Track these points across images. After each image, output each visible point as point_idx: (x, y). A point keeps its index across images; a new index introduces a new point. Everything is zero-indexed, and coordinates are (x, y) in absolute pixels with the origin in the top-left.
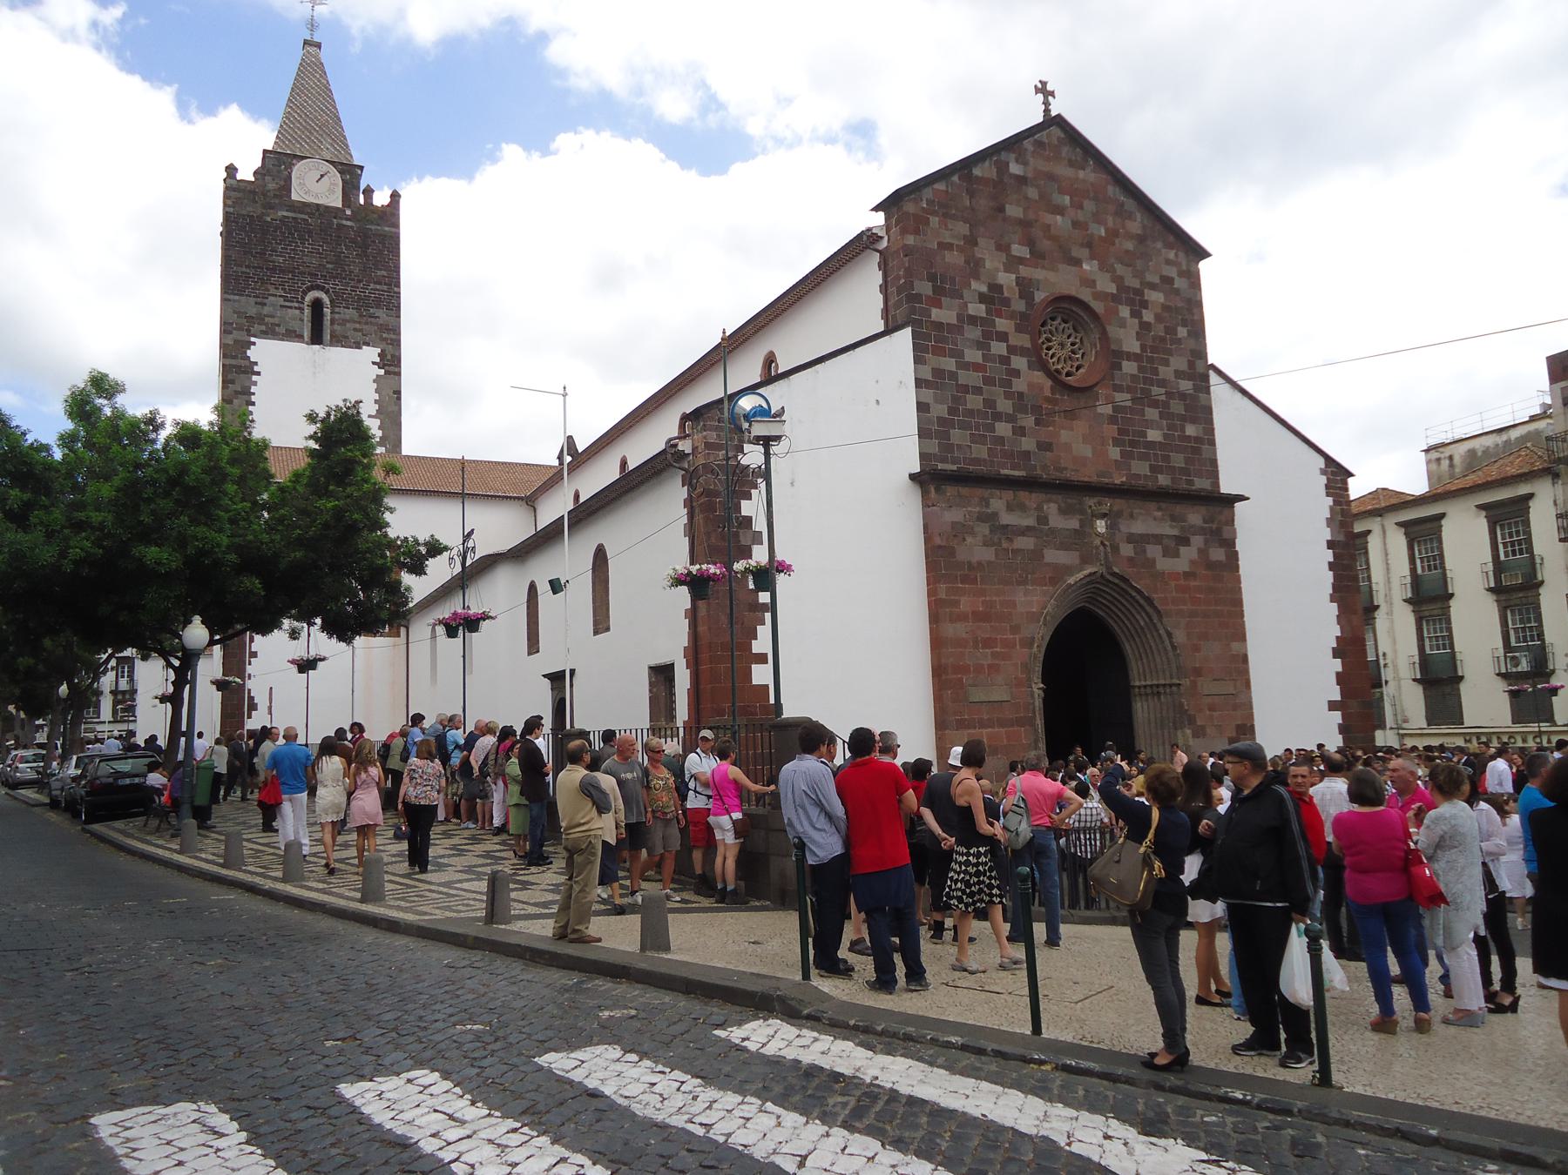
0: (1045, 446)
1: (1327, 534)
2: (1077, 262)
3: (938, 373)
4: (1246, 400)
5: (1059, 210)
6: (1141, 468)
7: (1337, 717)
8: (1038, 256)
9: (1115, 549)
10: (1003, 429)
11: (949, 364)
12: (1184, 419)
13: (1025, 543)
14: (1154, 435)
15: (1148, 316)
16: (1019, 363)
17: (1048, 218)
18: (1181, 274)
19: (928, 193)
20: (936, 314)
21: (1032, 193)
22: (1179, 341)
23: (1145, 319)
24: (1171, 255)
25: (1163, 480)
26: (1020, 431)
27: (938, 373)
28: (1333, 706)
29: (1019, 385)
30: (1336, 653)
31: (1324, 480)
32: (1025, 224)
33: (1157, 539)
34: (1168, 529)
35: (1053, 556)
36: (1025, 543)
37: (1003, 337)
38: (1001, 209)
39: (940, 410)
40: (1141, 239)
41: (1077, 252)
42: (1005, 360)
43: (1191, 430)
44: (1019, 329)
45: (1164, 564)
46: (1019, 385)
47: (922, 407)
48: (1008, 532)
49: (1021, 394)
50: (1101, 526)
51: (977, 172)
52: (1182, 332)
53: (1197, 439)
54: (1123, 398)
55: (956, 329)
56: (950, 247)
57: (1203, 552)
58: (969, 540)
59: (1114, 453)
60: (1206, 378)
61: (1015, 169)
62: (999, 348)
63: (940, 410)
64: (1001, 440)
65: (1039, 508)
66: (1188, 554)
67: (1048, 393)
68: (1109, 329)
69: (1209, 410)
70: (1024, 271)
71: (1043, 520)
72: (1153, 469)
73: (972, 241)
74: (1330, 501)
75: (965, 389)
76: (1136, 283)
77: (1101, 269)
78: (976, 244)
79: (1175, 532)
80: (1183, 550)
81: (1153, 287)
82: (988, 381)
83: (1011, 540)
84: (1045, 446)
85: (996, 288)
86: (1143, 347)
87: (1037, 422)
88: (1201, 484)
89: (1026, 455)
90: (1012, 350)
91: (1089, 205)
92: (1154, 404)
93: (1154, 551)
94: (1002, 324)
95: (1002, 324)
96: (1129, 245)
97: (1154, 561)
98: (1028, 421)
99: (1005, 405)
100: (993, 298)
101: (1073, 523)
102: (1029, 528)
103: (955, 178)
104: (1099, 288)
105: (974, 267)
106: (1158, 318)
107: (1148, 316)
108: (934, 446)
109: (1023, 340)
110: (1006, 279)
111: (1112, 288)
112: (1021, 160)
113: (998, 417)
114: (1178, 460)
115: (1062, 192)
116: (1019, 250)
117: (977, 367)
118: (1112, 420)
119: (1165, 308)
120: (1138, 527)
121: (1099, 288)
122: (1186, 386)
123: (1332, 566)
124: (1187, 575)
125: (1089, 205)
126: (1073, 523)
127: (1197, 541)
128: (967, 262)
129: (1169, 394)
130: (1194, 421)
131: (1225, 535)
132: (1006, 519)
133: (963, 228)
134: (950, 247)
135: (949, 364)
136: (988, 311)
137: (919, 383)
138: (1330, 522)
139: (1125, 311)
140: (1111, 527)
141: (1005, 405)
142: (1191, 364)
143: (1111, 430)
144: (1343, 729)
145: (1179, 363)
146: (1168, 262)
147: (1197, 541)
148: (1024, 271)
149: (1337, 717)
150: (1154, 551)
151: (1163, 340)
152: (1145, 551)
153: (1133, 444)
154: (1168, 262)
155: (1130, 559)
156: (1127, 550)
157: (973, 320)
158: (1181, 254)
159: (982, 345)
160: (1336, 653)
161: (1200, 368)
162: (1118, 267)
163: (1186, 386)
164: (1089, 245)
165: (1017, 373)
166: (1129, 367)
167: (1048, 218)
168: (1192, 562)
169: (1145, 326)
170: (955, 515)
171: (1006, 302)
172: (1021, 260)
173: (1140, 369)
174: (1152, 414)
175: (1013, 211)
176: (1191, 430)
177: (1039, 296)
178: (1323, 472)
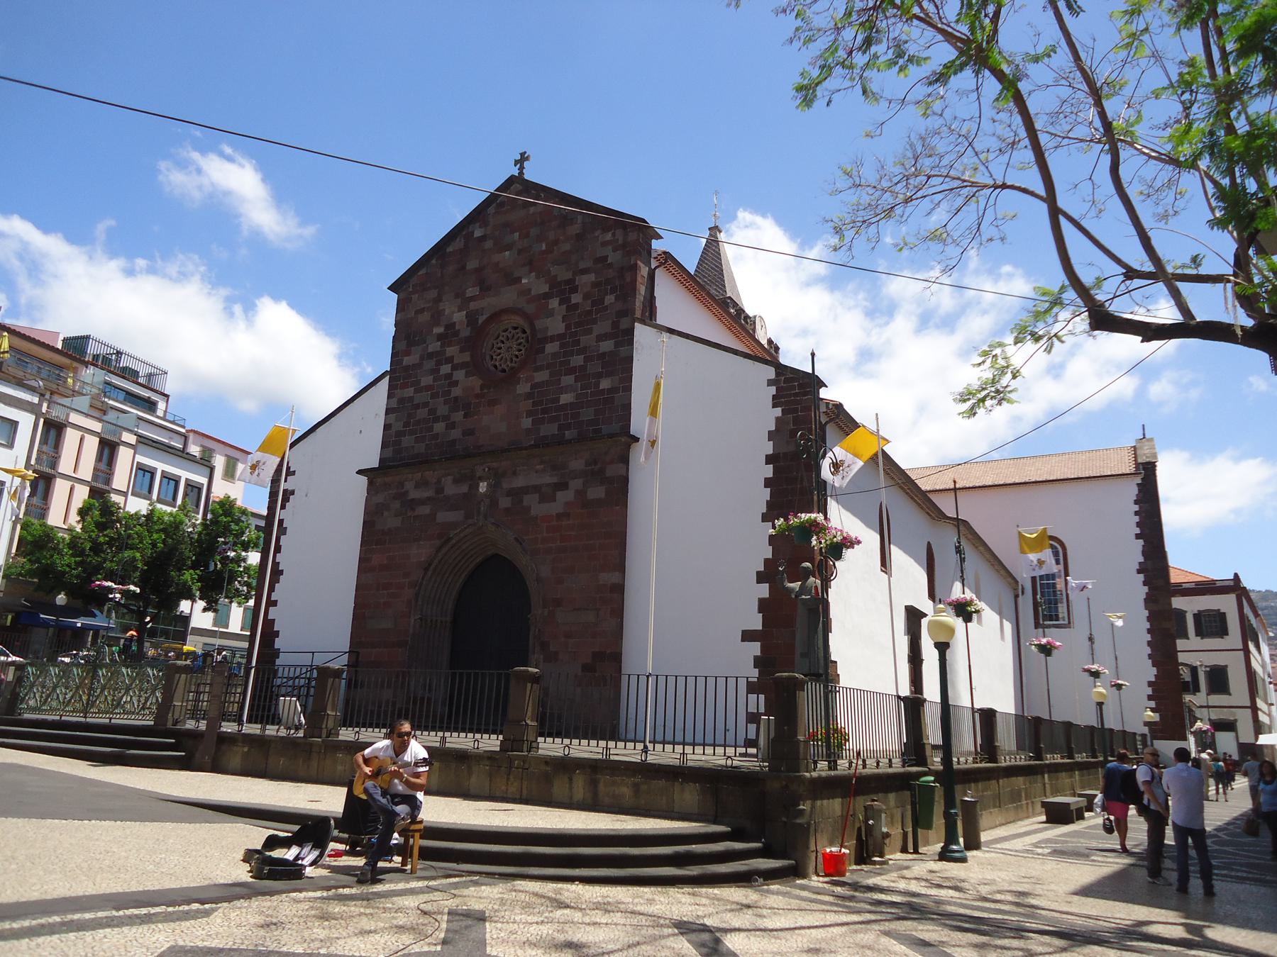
0: (469, 432)
1: (769, 448)
2: (519, 279)
3: (401, 401)
4: (675, 337)
5: (509, 247)
6: (550, 429)
7: (755, 648)
8: (485, 288)
9: (494, 503)
10: (439, 427)
11: (410, 392)
12: (600, 376)
13: (425, 510)
14: (566, 398)
15: (576, 298)
16: (459, 375)
17: (496, 257)
18: (615, 250)
19: (414, 280)
20: (407, 361)
21: (488, 244)
22: (606, 308)
23: (573, 301)
24: (609, 236)
25: (568, 434)
26: (452, 426)
27: (401, 401)
28: (748, 636)
29: (457, 392)
30: (761, 578)
31: (773, 390)
32: (478, 270)
33: (536, 489)
34: (548, 479)
35: (444, 516)
36: (425, 510)
37: (450, 360)
38: (463, 267)
39: (398, 426)
40: (580, 237)
41: (516, 275)
42: (449, 376)
43: (605, 384)
44: (462, 351)
45: (538, 509)
46: (457, 392)
47: (387, 427)
48: (413, 503)
49: (456, 398)
50: (483, 487)
51: (450, 249)
52: (610, 299)
53: (611, 391)
54: (541, 376)
55: (419, 365)
56: (422, 311)
57: (580, 494)
58: (386, 513)
59: (527, 423)
60: (630, 332)
61: (478, 233)
62: (445, 369)
63: (398, 426)
64: (436, 436)
65: (439, 481)
66: (564, 497)
67: (478, 391)
68: (539, 324)
69: (630, 359)
70: (473, 306)
71: (440, 490)
72: (560, 428)
73: (438, 300)
74: (778, 412)
75: (417, 407)
76: (568, 275)
77: (538, 277)
78: (441, 300)
79: (555, 480)
80: (560, 495)
81: (585, 271)
82: (434, 396)
83: (413, 510)
84: (469, 432)
85: (450, 326)
86: (568, 327)
87: (466, 416)
88: (605, 429)
89: (454, 441)
90: (454, 368)
91: (534, 231)
92: (571, 371)
93: (530, 500)
94: (451, 351)
95: (451, 351)
96: (566, 247)
97: (529, 508)
98: (458, 416)
99: (442, 410)
100: (450, 333)
101: (464, 489)
102: (429, 499)
103: (434, 261)
104: (533, 293)
105: (437, 317)
106: (586, 297)
107: (576, 298)
108: (389, 452)
109: (466, 357)
110: (459, 317)
111: (545, 288)
112: (484, 224)
113: (436, 420)
114: (587, 414)
115: (513, 232)
116: (471, 291)
117: (428, 388)
118: (529, 396)
119: (595, 285)
120: (519, 482)
121: (533, 293)
122: (607, 346)
123: (768, 483)
124: (559, 516)
125: (534, 231)
126: (464, 489)
127: (576, 484)
128: (432, 316)
129: (587, 359)
130: (609, 374)
131: (611, 471)
132: (414, 494)
133: (433, 294)
134: (422, 311)
135: (410, 392)
136: (442, 346)
137: (388, 412)
138: (771, 436)
139: (554, 303)
140: (493, 487)
141: (442, 410)
142: (615, 325)
143: (526, 405)
144: (758, 662)
145: (603, 327)
146: (604, 244)
147: (576, 484)
148: (473, 306)
149: (755, 648)
150: (530, 500)
151: (590, 312)
152: (522, 501)
153: (544, 411)
154: (604, 244)
155: (507, 510)
156: (505, 502)
157: (431, 355)
158: (619, 233)
159: (435, 371)
160: (761, 578)
161: (624, 324)
162: (554, 270)
163: (607, 346)
164: (531, 265)
165: (456, 383)
166: (551, 348)
167: (496, 257)
168: (567, 504)
169: (572, 308)
170: (380, 498)
171: (456, 333)
172: (472, 299)
173: (562, 346)
174: (568, 380)
175: (472, 265)
176: (605, 384)
177: (481, 320)
178: (770, 383)
